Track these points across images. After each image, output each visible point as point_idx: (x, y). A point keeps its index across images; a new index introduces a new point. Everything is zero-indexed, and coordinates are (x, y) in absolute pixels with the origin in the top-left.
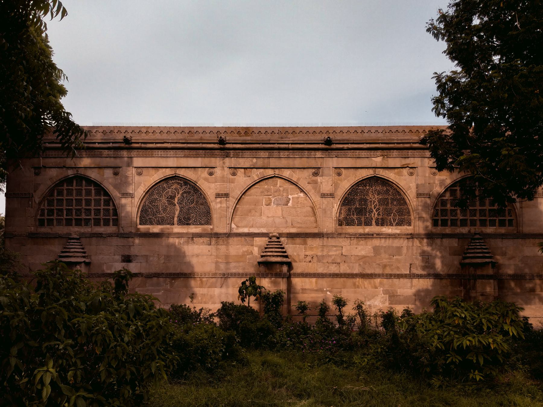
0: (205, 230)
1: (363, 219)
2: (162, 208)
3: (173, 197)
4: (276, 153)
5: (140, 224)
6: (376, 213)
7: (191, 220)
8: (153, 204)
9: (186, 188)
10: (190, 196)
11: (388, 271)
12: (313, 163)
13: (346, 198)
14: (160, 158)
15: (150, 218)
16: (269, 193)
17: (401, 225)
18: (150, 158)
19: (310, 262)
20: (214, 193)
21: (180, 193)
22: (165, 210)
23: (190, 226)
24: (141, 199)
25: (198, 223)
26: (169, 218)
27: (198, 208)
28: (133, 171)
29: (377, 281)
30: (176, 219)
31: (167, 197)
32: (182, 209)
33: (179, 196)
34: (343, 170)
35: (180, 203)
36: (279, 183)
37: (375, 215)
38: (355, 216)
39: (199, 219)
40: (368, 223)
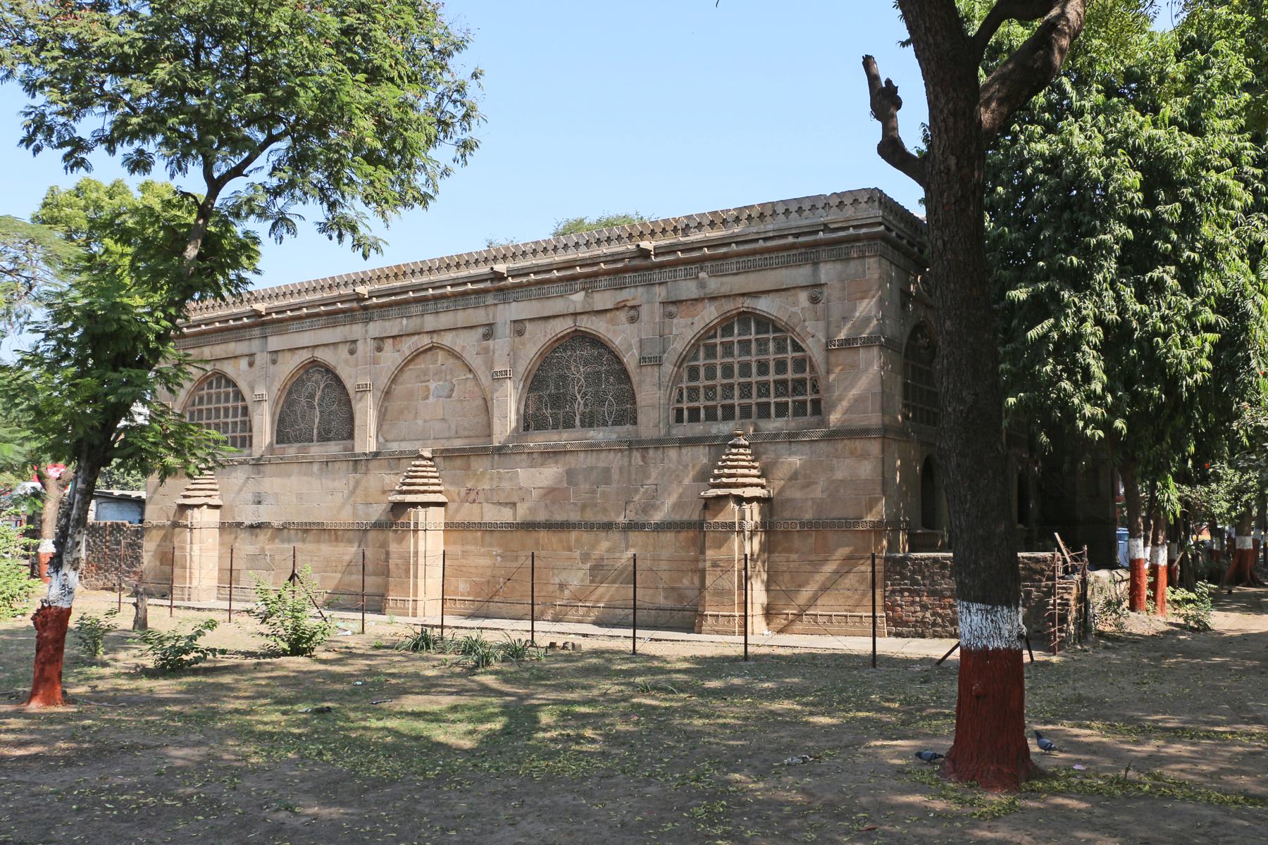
1: (561, 417)
3: (312, 396)
4: (431, 306)
5: (277, 443)
6: (582, 402)
11: (590, 516)
12: (479, 316)
13: (535, 376)
16: (427, 378)
17: (620, 424)
19: (474, 501)
22: (303, 417)
29: (574, 535)
30: (315, 431)
34: (527, 324)
35: (320, 405)
36: (440, 357)
37: (579, 406)
38: (549, 411)
40: (569, 424)
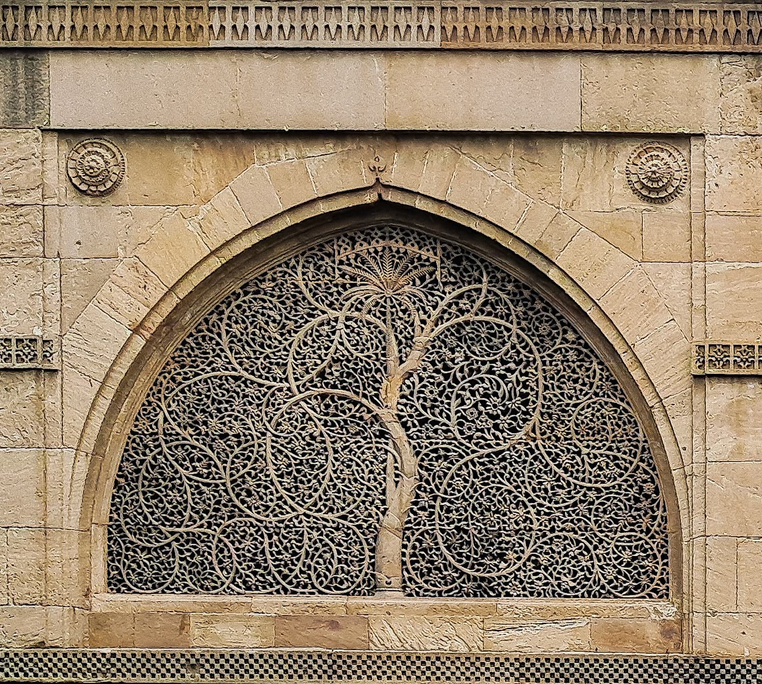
0: (617, 634)
2: (282, 462)
5: (116, 584)
7: (511, 555)
8: (213, 422)
9: (464, 303)
10: (499, 368)
14: (256, 62)
15: (192, 538)
18: (177, 65)
20: (682, 345)
21: (421, 339)
23: (503, 602)
24: (110, 394)
25: (568, 582)
26: (339, 535)
27: (564, 459)
28: (51, 164)
31: (322, 375)
32: (439, 466)
33: (409, 365)
39: (573, 550)
